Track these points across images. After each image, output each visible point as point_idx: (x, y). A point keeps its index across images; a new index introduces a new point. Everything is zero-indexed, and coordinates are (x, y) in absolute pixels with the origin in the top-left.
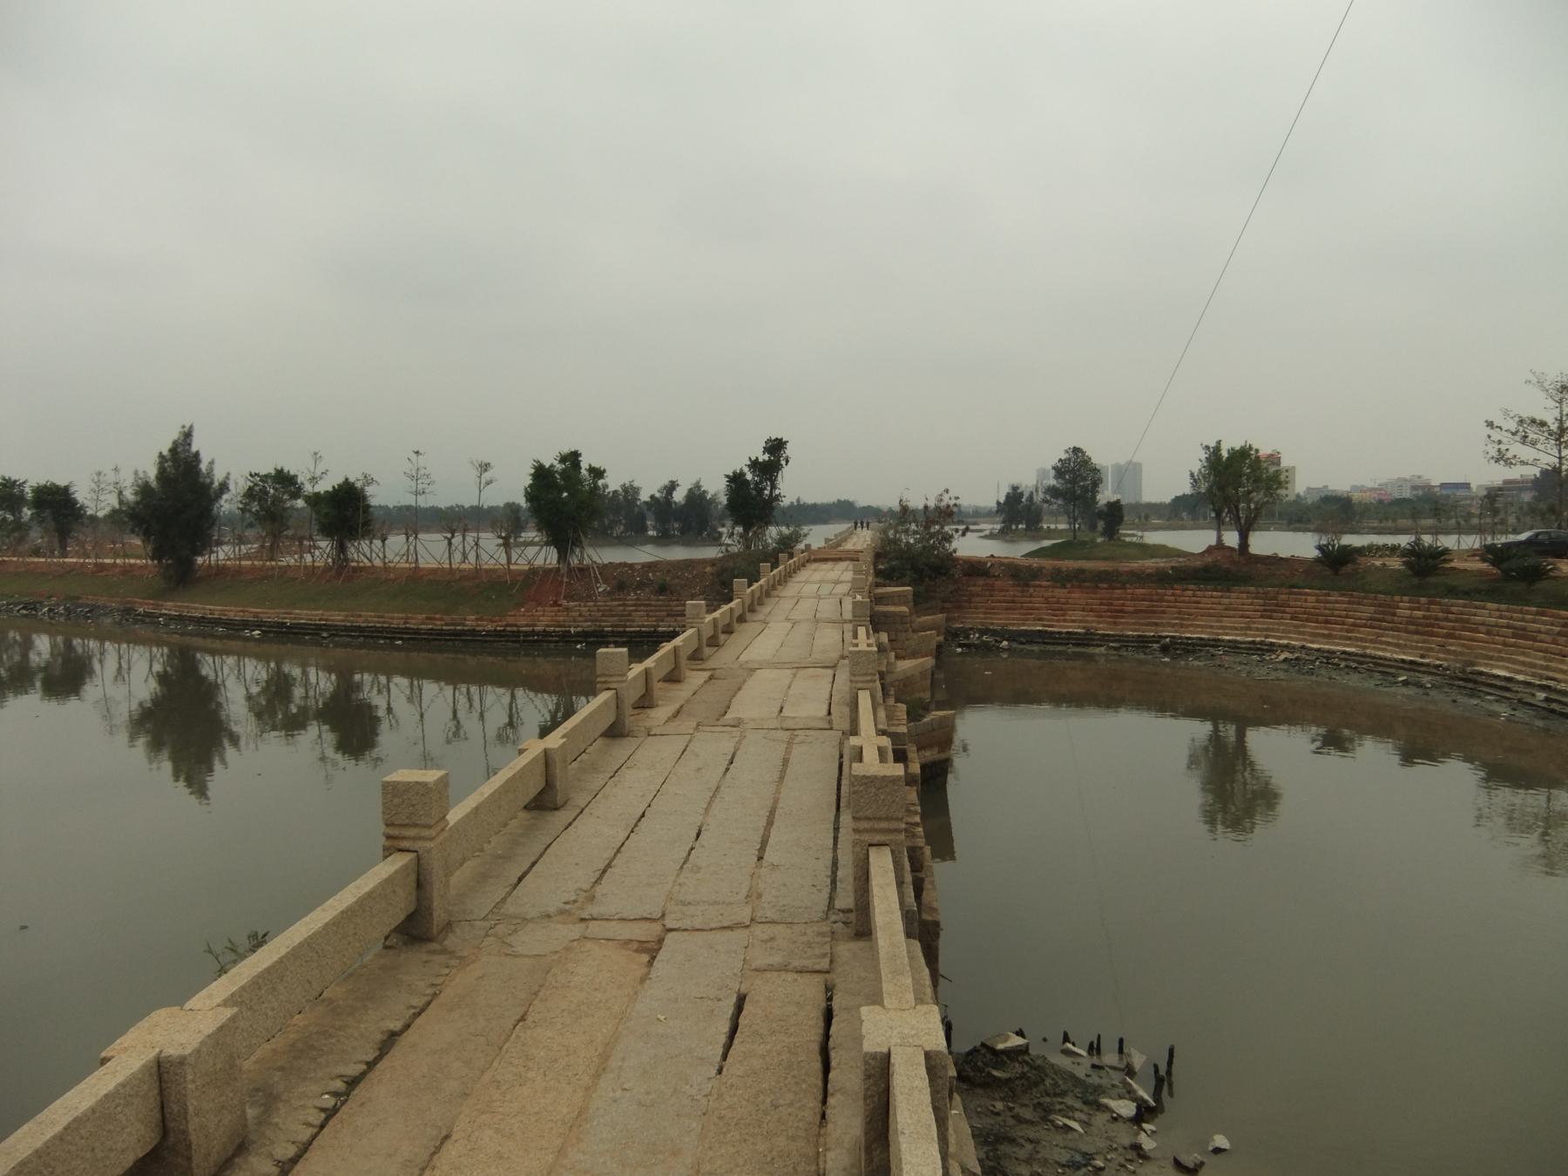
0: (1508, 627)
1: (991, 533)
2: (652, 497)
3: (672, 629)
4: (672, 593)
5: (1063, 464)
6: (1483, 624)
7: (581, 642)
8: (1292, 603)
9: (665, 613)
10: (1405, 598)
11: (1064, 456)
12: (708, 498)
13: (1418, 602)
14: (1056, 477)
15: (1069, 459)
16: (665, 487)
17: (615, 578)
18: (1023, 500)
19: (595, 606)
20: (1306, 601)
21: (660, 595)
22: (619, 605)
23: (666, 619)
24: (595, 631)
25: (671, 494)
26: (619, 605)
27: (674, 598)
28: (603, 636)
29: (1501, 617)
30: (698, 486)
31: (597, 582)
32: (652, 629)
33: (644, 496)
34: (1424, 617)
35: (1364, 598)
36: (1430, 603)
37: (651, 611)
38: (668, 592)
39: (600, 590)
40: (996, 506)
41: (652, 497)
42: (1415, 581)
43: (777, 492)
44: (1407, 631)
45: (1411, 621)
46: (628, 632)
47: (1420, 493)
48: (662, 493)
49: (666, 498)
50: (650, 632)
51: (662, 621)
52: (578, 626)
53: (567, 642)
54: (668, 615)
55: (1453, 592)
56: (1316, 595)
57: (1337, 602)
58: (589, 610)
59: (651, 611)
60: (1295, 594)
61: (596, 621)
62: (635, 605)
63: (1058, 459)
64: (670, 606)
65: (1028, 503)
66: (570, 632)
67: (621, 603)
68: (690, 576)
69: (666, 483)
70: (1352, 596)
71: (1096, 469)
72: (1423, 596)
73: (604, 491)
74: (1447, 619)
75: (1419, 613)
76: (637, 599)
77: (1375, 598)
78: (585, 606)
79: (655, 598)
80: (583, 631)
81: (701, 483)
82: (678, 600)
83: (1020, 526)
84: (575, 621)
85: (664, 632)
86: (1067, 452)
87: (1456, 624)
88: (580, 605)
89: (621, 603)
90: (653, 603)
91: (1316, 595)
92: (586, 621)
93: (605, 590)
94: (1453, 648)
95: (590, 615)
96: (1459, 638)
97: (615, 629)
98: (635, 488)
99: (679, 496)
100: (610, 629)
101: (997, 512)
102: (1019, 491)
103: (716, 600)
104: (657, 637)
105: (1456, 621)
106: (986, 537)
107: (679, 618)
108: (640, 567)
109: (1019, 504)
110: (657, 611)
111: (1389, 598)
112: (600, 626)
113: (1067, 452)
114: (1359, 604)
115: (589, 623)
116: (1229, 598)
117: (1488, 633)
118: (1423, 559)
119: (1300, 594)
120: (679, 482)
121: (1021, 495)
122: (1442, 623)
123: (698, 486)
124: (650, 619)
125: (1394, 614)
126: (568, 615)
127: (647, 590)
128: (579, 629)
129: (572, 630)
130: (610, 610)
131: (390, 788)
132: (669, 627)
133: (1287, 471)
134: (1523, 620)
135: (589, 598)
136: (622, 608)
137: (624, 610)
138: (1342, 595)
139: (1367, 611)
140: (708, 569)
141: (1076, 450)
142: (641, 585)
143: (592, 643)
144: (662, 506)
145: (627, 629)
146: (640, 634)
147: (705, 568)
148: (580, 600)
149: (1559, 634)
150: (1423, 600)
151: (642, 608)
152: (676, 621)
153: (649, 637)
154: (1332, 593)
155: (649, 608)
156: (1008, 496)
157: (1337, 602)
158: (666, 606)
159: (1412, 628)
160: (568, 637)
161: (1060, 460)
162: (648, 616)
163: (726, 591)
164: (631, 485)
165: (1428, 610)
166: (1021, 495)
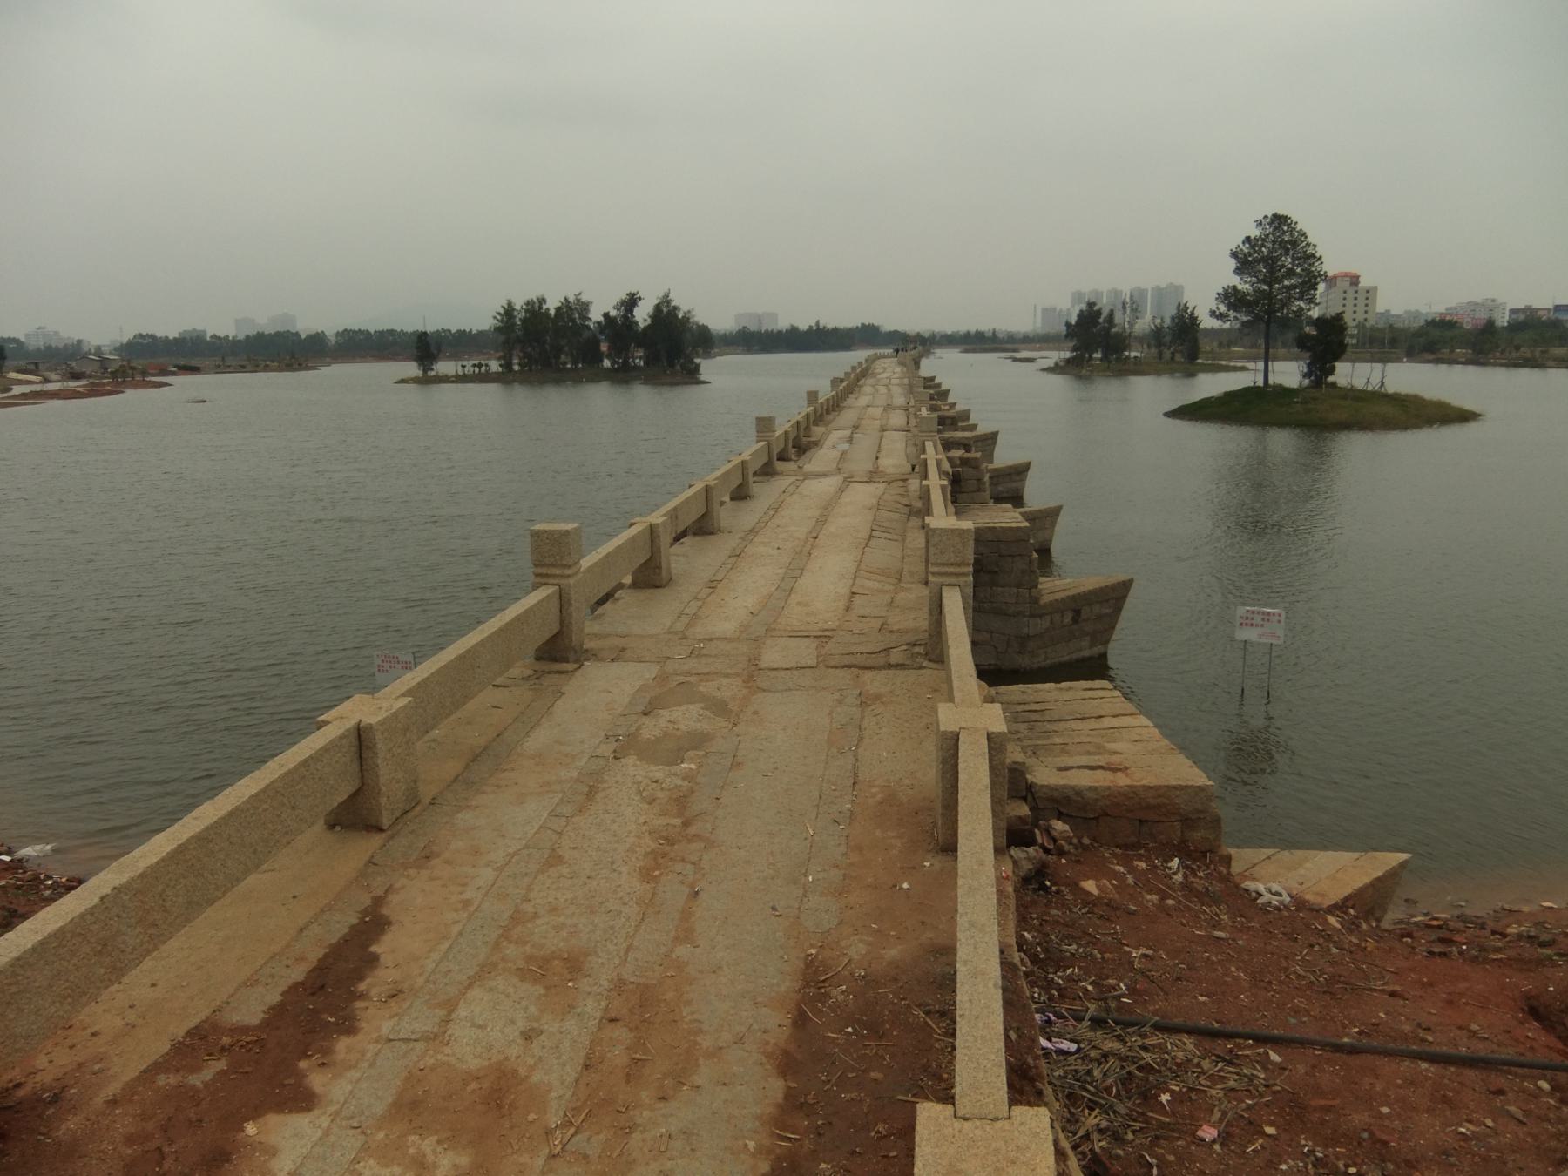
1: (1056, 364)
2: (606, 315)
5: (1252, 247)
11: (1255, 232)
12: (680, 316)
14: (1238, 271)
16: (623, 303)
18: (1101, 320)
25: (632, 311)
30: (666, 300)
33: (596, 315)
40: (1065, 328)
41: (606, 315)
47: (1522, 317)
48: (618, 310)
49: (625, 317)
63: (1243, 237)
65: (1106, 325)
69: (624, 296)
71: (1313, 256)
73: (540, 308)
81: (671, 297)
83: (1095, 355)
86: (1259, 223)
98: (583, 303)
99: (642, 315)
101: (1066, 336)
102: (1096, 308)
106: (1049, 370)
109: (1095, 327)
113: (1259, 223)
120: (640, 294)
121: (1099, 313)
123: (666, 300)
133: (1368, 292)
141: (1279, 220)
144: (620, 328)
156: (1081, 315)
161: (1248, 239)
164: (578, 300)
166: (1099, 313)
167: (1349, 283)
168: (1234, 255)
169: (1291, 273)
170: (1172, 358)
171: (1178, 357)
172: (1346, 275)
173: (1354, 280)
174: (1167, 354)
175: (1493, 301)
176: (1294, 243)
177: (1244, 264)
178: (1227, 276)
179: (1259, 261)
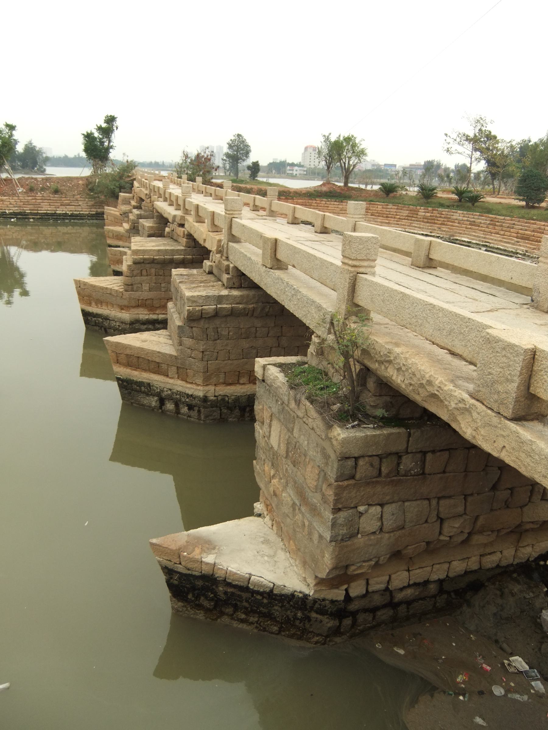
0: (467, 221)
3: (64, 212)
4: (62, 194)
6: (457, 219)
7: (13, 218)
8: (371, 208)
9: (59, 204)
10: (422, 208)
11: (233, 138)
13: (428, 209)
15: (235, 140)
17: (28, 185)
19: (18, 199)
20: (377, 208)
21: (56, 195)
22: (32, 199)
23: (60, 207)
24: (20, 212)
26: (32, 199)
27: (63, 196)
28: (25, 215)
29: (464, 217)
31: (18, 186)
32: (54, 212)
34: (431, 216)
35: (403, 207)
36: (433, 210)
37: (51, 203)
38: (60, 193)
39: (20, 191)
42: (424, 200)
43: (111, 144)
44: (423, 222)
45: (425, 217)
46: (40, 213)
50: (52, 214)
51: (58, 208)
52: (10, 210)
53: (4, 217)
54: (61, 205)
55: (442, 205)
56: (382, 205)
57: (391, 208)
58: (15, 201)
59: (51, 203)
60: (373, 204)
61: (20, 207)
62: (42, 199)
64: (61, 200)
66: (6, 213)
67: (33, 198)
68: (71, 185)
70: (398, 206)
71: (248, 145)
72: (430, 207)
74: (440, 217)
75: (429, 214)
76: (43, 196)
77: (409, 207)
78: (12, 199)
79: (53, 196)
80: (14, 212)
82: (65, 198)
84: (8, 207)
85: (60, 214)
87: (445, 219)
88: (9, 199)
89: (33, 198)
90: (52, 198)
91: (382, 205)
92: (14, 207)
93: (22, 191)
94: (444, 229)
95: (16, 204)
96: (446, 225)
97: (32, 211)
100: (29, 211)
103: (86, 198)
104: (57, 216)
105: (444, 218)
107: (68, 207)
108: (41, 180)
110: (55, 203)
111: (414, 207)
112: (23, 210)
114: (401, 209)
115: (17, 208)
116: (342, 205)
117: (459, 223)
118: (427, 191)
119: (375, 204)
122: (439, 219)
124: (51, 207)
125: (417, 214)
126: (3, 204)
127: (47, 192)
128: (11, 211)
129: (7, 211)
130: (27, 202)
131: (358, 239)
132: (63, 211)
134: (473, 218)
135: (14, 195)
136: (34, 201)
137: (36, 202)
138: (394, 205)
139: (405, 213)
140: (80, 182)
141: (239, 135)
142: (43, 189)
143: (20, 218)
145: (39, 212)
146: (47, 214)
147: (78, 181)
148: (9, 195)
149: (489, 224)
150: (430, 209)
151: (46, 201)
152: (66, 208)
153: (53, 216)
154: (389, 204)
155: (50, 201)
157: (391, 208)
158: (60, 200)
159: (426, 220)
160: (6, 215)
162: (50, 205)
163: (92, 194)
165: (432, 213)
167: (312, 150)
168: (228, 144)
169: (243, 150)
170: (230, 175)
171: (232, 174)
172: (311, 147)
173: (314, 149)
174: (228, 173)
175: (374, 161)
176: (243, 142)
177: (230, 147)
178: (226, 150)
179: (234, 146)
